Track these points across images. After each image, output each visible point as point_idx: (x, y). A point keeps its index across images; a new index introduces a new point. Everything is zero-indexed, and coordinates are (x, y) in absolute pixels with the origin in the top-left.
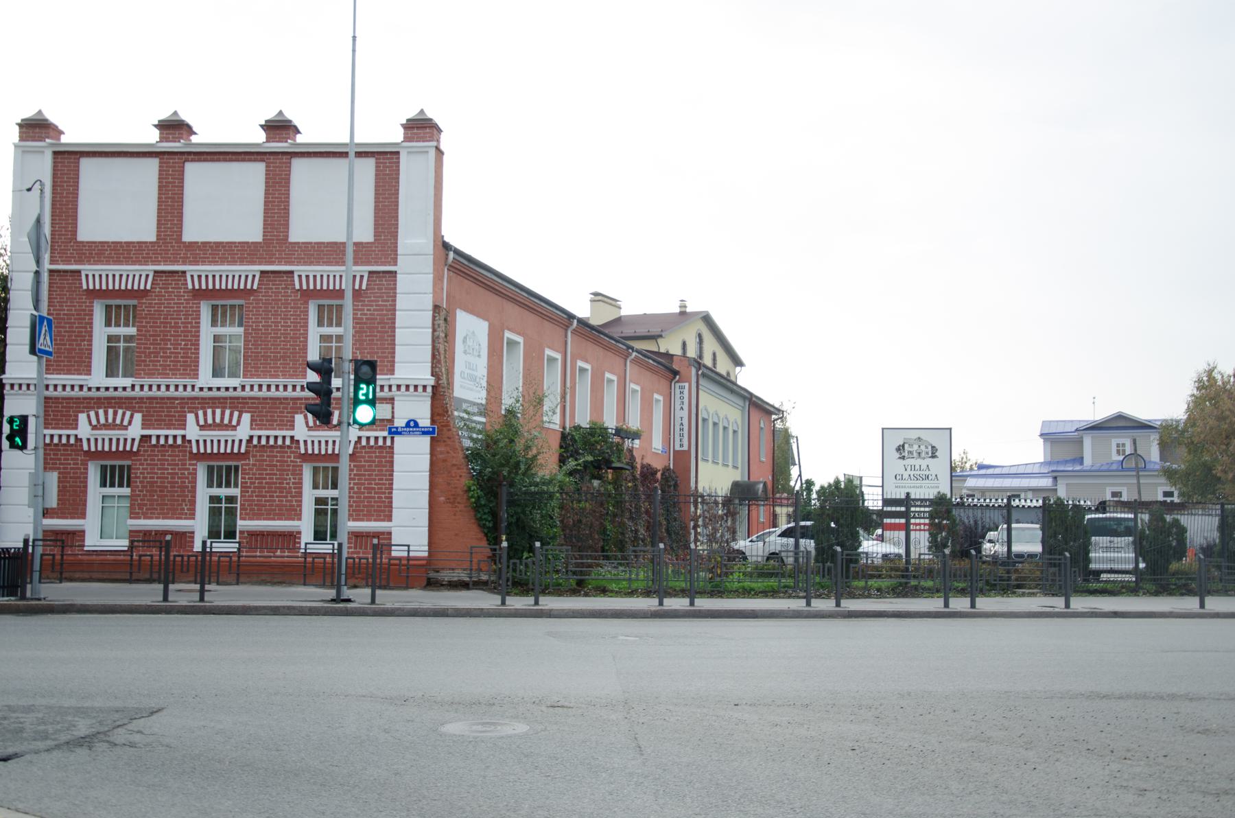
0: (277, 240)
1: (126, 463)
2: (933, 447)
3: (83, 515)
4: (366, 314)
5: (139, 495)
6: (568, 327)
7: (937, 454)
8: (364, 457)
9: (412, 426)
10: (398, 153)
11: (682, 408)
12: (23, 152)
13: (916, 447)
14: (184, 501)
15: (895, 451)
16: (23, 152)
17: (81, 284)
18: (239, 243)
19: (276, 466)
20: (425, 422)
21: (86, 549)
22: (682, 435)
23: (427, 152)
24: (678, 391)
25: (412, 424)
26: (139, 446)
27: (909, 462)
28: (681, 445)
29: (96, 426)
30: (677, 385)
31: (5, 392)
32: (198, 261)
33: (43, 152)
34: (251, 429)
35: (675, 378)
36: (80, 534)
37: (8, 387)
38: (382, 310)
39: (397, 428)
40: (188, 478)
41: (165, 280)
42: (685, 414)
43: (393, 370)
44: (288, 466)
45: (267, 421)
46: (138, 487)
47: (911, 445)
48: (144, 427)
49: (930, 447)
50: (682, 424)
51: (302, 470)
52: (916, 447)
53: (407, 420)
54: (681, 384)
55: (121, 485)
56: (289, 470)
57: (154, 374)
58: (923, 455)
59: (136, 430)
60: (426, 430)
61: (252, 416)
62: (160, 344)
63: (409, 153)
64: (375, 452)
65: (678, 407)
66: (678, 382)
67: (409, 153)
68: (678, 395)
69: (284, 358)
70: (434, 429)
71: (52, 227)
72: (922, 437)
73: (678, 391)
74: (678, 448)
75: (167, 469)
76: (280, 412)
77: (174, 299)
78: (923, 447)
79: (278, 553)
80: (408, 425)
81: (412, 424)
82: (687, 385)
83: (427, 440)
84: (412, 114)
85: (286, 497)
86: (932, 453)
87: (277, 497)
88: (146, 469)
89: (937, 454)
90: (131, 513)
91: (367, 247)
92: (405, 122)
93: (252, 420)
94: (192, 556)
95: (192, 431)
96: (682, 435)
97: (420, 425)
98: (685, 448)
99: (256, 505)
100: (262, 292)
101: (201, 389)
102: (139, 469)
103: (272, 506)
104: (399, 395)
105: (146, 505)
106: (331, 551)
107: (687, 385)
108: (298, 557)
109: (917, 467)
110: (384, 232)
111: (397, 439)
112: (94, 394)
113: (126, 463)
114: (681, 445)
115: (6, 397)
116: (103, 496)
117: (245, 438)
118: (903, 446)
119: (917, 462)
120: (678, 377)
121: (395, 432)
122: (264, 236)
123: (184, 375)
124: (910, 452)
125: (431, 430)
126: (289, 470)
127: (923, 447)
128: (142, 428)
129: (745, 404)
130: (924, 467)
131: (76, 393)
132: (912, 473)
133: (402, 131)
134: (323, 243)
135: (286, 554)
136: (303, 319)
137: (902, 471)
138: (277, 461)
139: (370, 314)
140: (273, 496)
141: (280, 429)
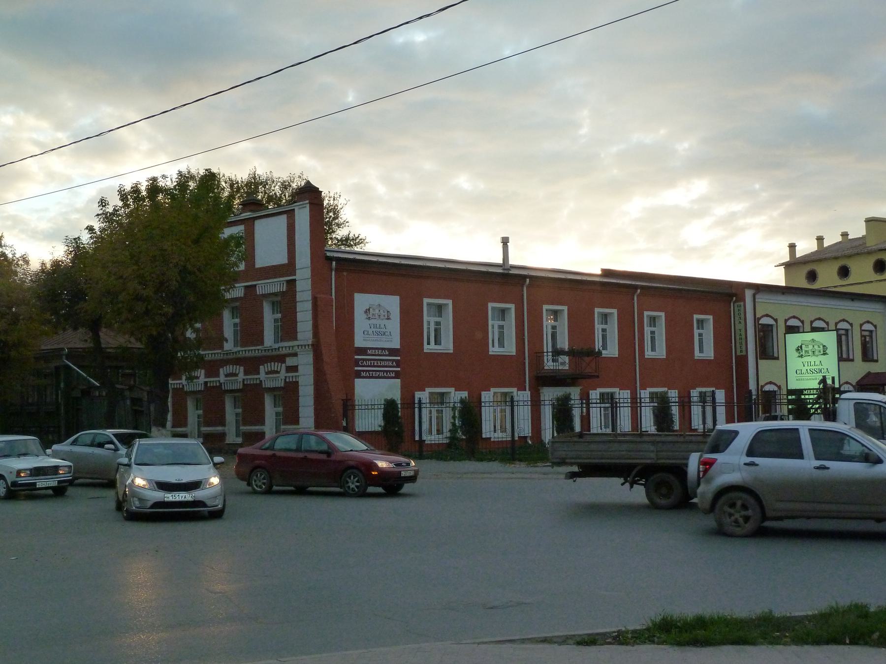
2: (824, 346)
7: (827, 352)
11: (740, 322)
13: (811, 347)
15: (795, 352)
24: (736, 309)
27: (806, 359)
30: (736, 305)
42: (742, 326)
47: (807, 346)
49: (821, 347)
50: (741, 335)
52: (811, 347)
54: (738, 304)
58: (817, 353)
63: (299, 208)
65: (737, 322)
66: (734, 303)
72: (815, 339)
74: (739, 353)
78: (816, 347)
86: (824, 351)
89: (827, 352)
98: (744, 353)
107: (742, 304)
109: (813, 363)
114: (741, 351)
118: (801, 347)
119: (812, 359)
120: (734, 298)
124: (806, 351)
127: (816, 347)
130: (817, 363)
132: (809, 368)
137: (801, 367)
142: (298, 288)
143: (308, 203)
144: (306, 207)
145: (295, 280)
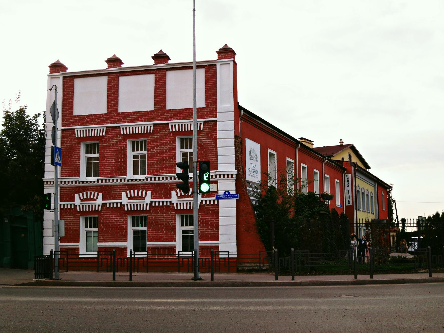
0: (161, 109)
1: (96, 216)
3: (78, 241)
4: (203, 142)
5: (102, 231)
6: (297, 147)
8: (205, 210)
9: (227, 195)
10: (216, 65)
11: (348, 186)
12: (51, 78)
14: (122, 233)
16: (51, 78)
17: (75, 135)
18: (144, 111)
19: (163, 216)
20: (233, 192)
21: (80, 256)
22: (349, 199)
23: (229, 63)
24: (346, 178)
25: (227, 193)
26: (102, 208)
28: (349, 203)
29: (82, 199)
30: (346, 175)
31: (44, 185)
32: (126, 121)
33: (59, 77)
34: (152, 198)
35: (345, 172)
36: (77, 250)
37: (45, 183)
38: (211, 139)
39: (220, 195)
40: (123, 222)
41: (111, 131)
42: (350, 188)
43: (217, 168)
44: (169, 215)
45: (159, 194)
46: (101, 227)
48: (103, 199)
50: (349, 193)
51: (175, 217)
53: (224, 192)
55: (94, 227)
56: (170, 218)
57: (107, 175)
59: (100, 201)
60: (234, 196)
61: (152, 192)
62: (109, 161)
63: (220, 64)
64: (210, 208)
65: (346, 185)
66: (346, 174)
67: (220, 64)
68: (346, 180)
69: (165, 164)
70: (237, 195)
71: (63, 110)
73: (346, 178)
74: (347, 204)
75: (114, 219)
76: (165, 190)
77: (115, 140)
79: (166, 257)
80: (225, 193)
81: (227, 193)
82: (350, 175)
83: (233, 202)
84: (221, 46)
85: (169, 230)
87: (164, 230)
88: (105, 219)
90: (99, 240)
91: (203, 110)
92: (218, 50)
93: (152, 195)
94: (126, 259)
95: (125, 200)
96: (349, 199)
97: (231, 194)
98: (351, 204)
99: (155, 234)
100: (154, 134)
101: (128, 180)
102: (102, 219)
103: (162, 234)
104: (219, 180)
105: (105, 236)
106: (191, 256)
107: (350, 175)
108: (175, 259)
110: (210, 102)
111: (220, 201)
112: (81, 185)
113: (96, 216)
114: (349, 203)
115: (45, 188)
116: (87, 232)
117: (149, 203)
121: (219, 197)
122: (155, 107)
123: (120, 175)
125: (236, 196)
126: (170, 218)
128: (103, 200)
129: (375, 184)
131: (74, 185)
133: (217, 55)
134: (182, 109)
135: (170, 258)
136: (174, 145)
138: (164, 213)
139: (205, 142)
140: (162, 230)
141: (165, 198)
142: (219, 128)
143: (232, 61)
144: (229, 63)
145: (216, 121)
